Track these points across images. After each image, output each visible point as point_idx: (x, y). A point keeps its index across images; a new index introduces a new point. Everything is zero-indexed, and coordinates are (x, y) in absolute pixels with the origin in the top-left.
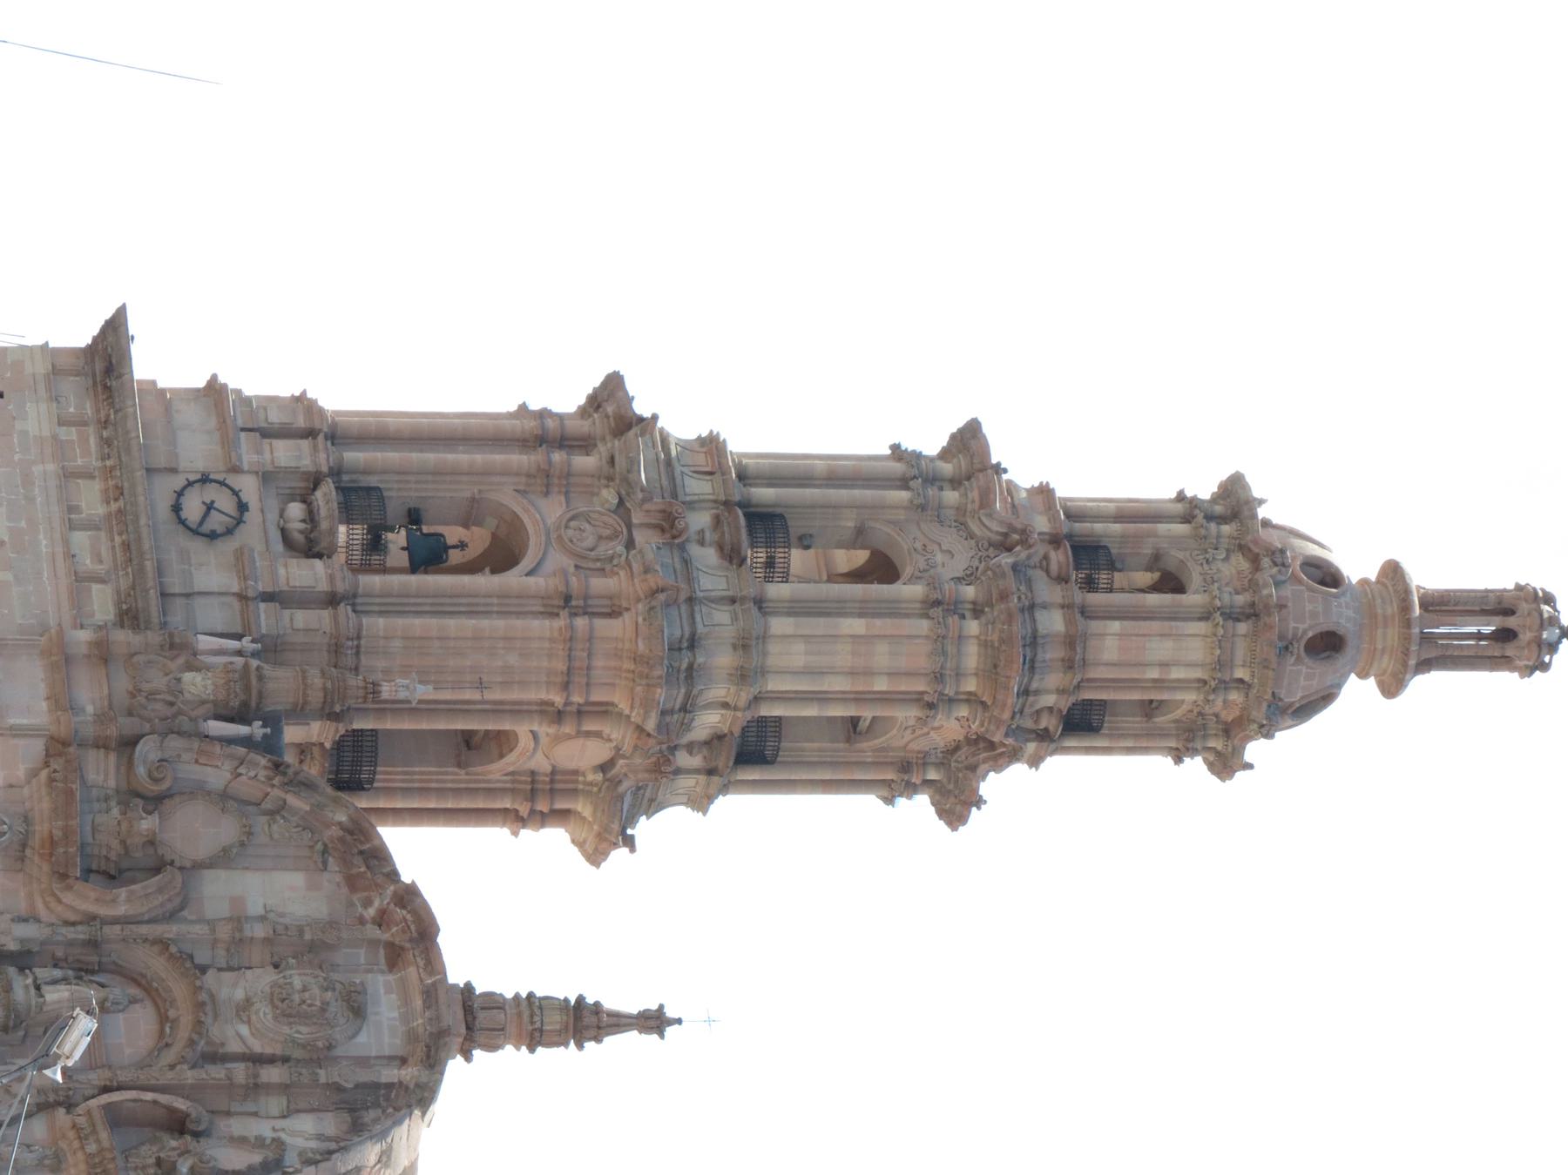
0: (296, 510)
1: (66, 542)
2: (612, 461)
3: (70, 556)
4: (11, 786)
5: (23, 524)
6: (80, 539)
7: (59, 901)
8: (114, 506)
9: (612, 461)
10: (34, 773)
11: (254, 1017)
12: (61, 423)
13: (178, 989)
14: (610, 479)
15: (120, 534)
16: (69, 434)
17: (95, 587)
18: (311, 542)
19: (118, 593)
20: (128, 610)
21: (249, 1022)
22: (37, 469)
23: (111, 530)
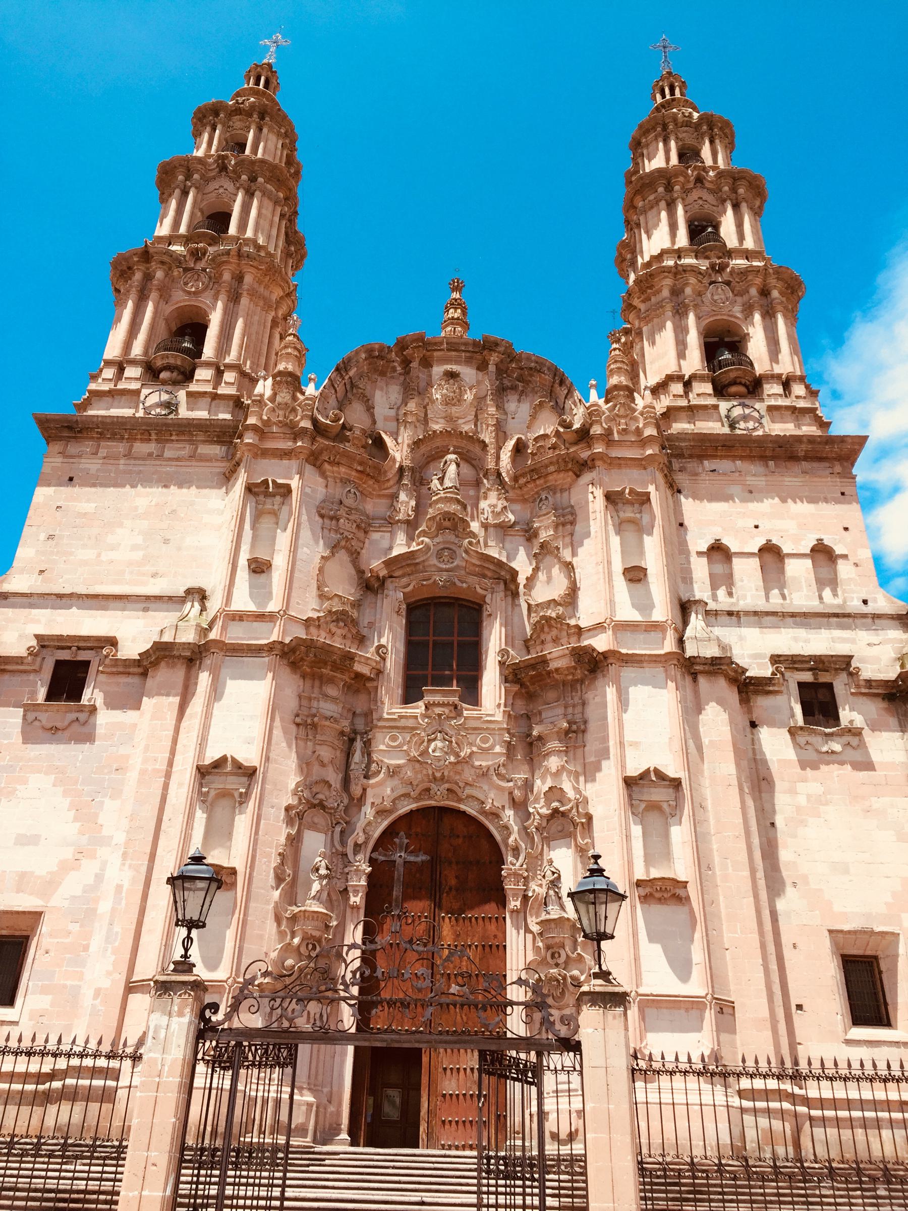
0: (164, 375)
1: (170, 459)
2: (162, 263)
3: (178, 459)
4: (327, 486)
5: (155, 477)
6: (168, 454)
7: (388, 480)
8: (154, 437)
9: (162, 263)
10: (323, 474)
11: (457, 415)
12: (96, 453)
13: (438, 443)
14: (170, 269)
15: (171, 435)
16: (103, 452)
17: (199, 451)
18: (183, 373)
19: (204, 442)
20: (218, 436)
21: (458, 418)
22: (121, 467)
23: (167, 441)
